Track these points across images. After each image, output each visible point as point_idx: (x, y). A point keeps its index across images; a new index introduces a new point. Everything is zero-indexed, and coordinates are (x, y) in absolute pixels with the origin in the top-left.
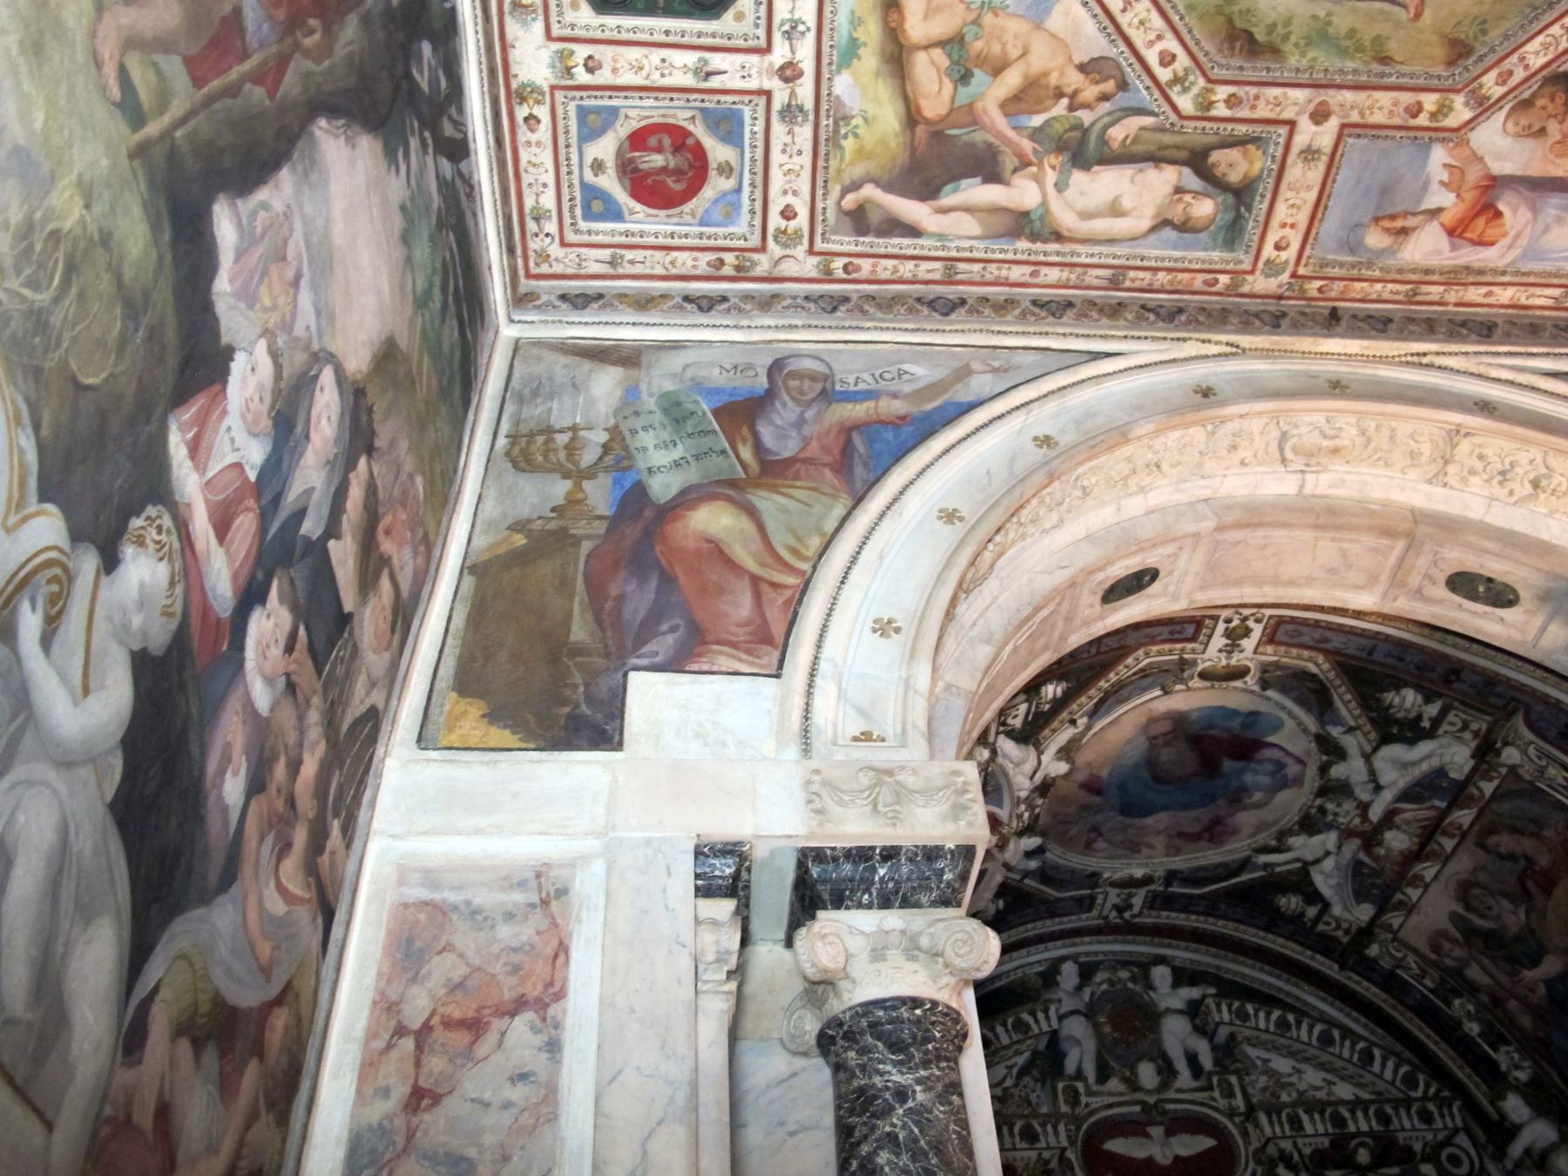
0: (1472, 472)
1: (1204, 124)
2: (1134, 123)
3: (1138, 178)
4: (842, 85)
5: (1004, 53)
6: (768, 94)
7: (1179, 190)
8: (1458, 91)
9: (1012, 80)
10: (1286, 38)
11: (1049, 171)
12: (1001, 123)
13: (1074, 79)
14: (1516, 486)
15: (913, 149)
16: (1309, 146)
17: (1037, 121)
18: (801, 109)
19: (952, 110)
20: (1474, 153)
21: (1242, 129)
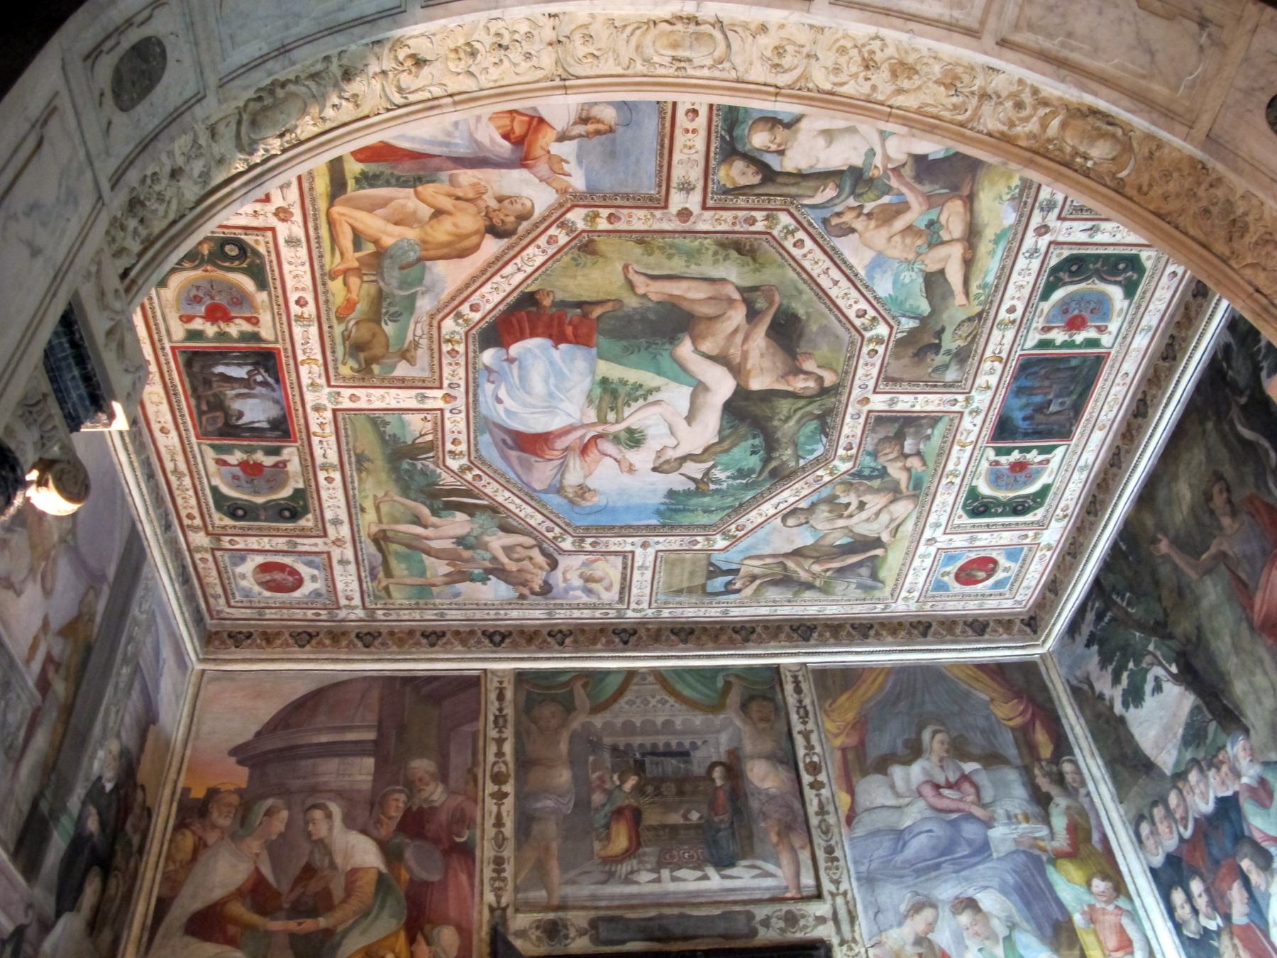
0: (529, 35)
1: (770, 206)
2: (819, 199)
3: (814, 161)
4: (1010, 218)
5: (903, 238)
6: (1059, 218)
7: (781, 153)
8: (584, 231)
9: (900, 224)
10: (715, 253)
11: (879, 165)
12: (910, 197)
13: (859, 224)
14: (489, 40)
15: (973, 180)
16: (688, 193)
17: (886, 199)
18: (1042, 209)
19: (943, 205)
20: (548, 184)
21: (741, 201)
